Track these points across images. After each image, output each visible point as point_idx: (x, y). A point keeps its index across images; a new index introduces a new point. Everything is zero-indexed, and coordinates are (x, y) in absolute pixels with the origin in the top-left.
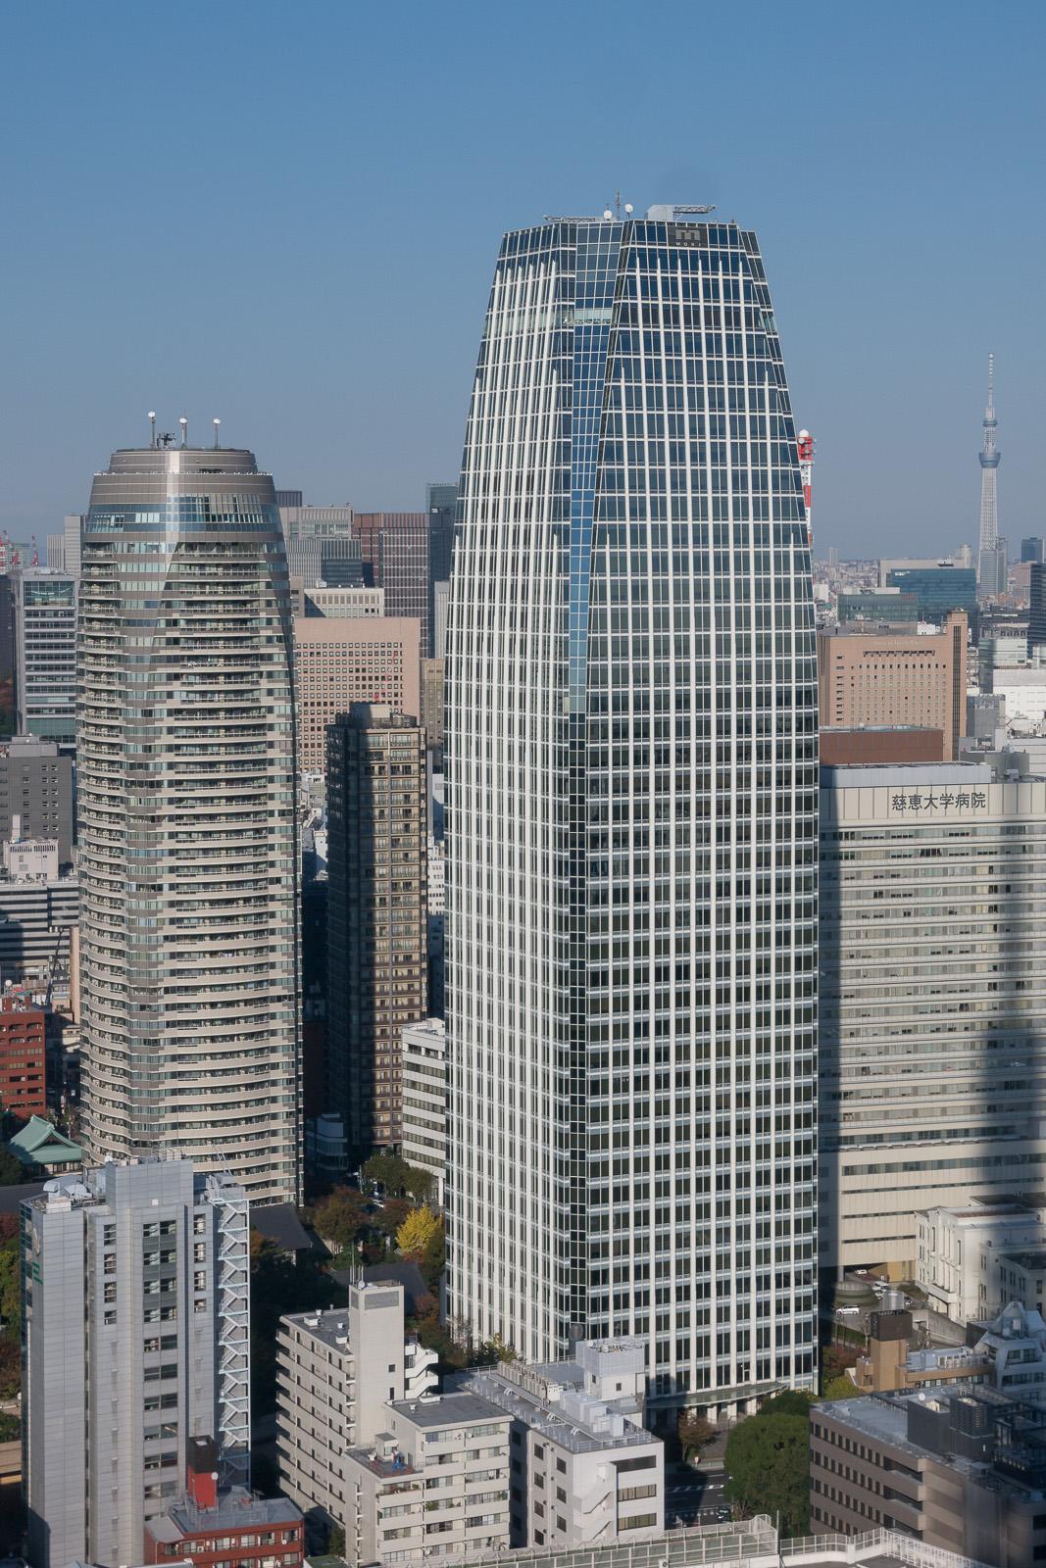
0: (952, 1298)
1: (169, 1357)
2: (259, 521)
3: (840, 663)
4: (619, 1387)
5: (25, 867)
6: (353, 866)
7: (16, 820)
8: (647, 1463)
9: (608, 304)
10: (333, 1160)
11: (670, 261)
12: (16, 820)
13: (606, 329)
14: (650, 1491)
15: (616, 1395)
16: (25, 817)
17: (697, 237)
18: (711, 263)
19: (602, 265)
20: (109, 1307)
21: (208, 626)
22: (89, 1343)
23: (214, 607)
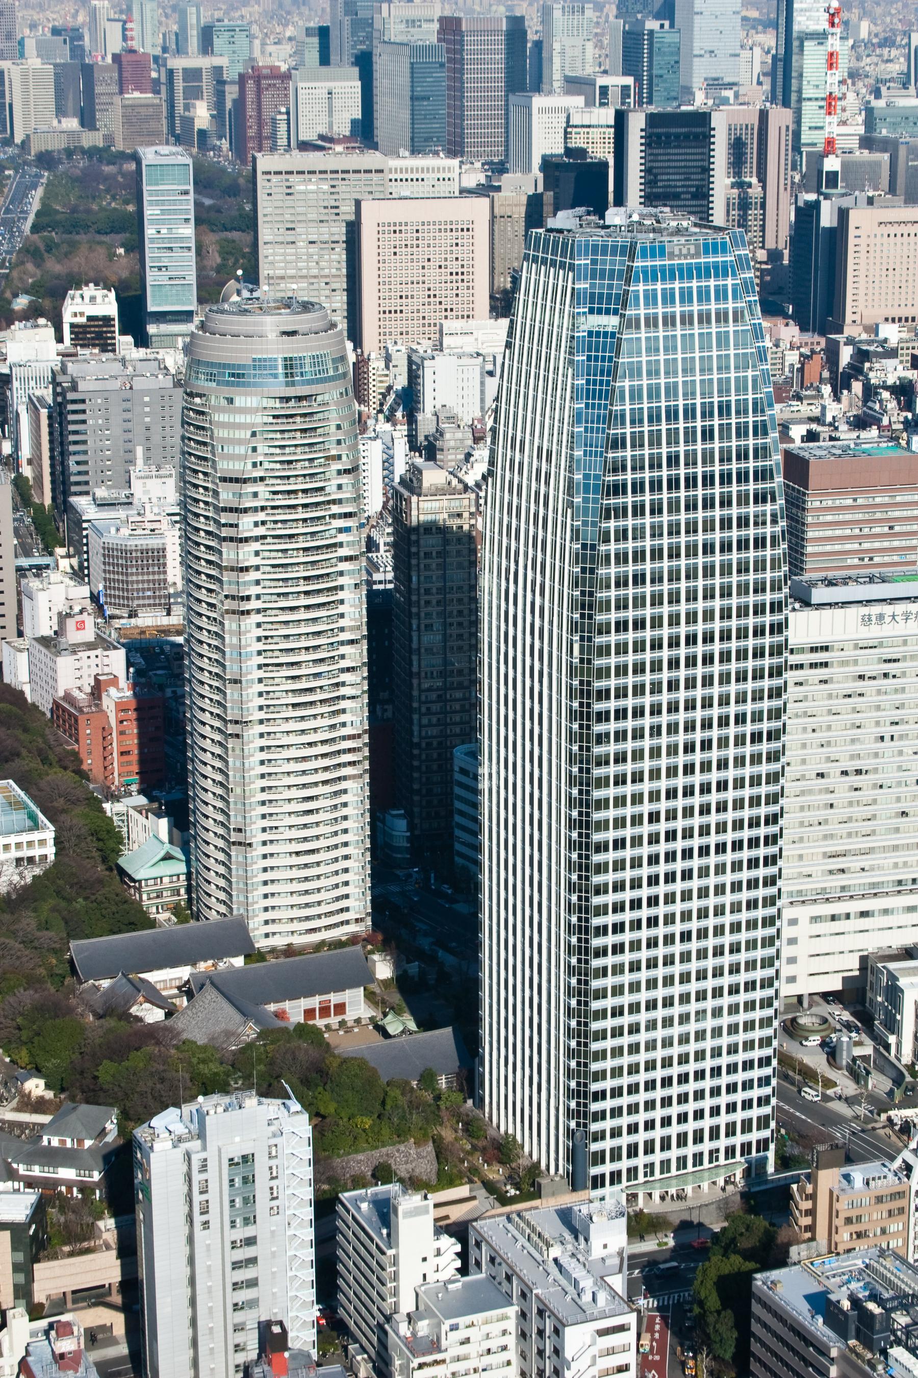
0: (892, 1039)
1: (249, 1252)
2: (331, 373)
3: (858, 233)
4: (605, 1246)
5: (148, 492)
6: (414, 598)
7: (139, 451)
8: (622, 1328)
9: (616, 312)
10: (398, 850)
11: (670, 274)
12: (139, 451)
13: (613, 334)
14: (625, 1349)
15: (604, 1253)
16: (149, 449)
17: (692, 251)
18: (704, 272)
19: (611, 278)
20: (205, 1218)
21: (287, 450)
22: (191, 1240)
23: (291, 435)
